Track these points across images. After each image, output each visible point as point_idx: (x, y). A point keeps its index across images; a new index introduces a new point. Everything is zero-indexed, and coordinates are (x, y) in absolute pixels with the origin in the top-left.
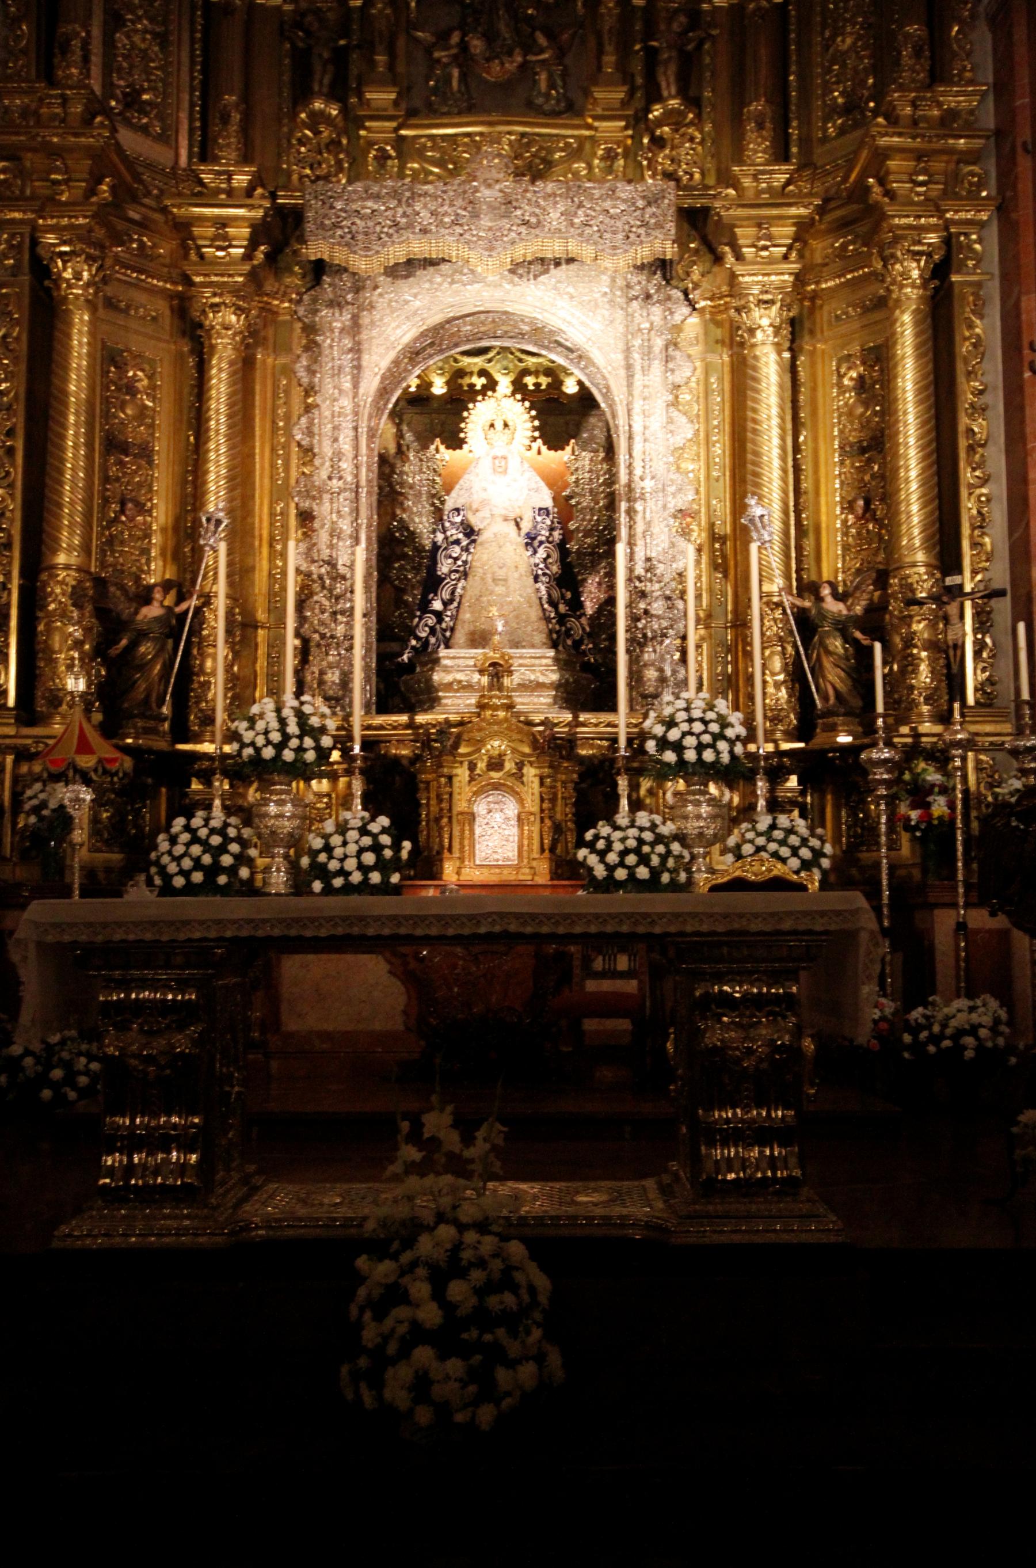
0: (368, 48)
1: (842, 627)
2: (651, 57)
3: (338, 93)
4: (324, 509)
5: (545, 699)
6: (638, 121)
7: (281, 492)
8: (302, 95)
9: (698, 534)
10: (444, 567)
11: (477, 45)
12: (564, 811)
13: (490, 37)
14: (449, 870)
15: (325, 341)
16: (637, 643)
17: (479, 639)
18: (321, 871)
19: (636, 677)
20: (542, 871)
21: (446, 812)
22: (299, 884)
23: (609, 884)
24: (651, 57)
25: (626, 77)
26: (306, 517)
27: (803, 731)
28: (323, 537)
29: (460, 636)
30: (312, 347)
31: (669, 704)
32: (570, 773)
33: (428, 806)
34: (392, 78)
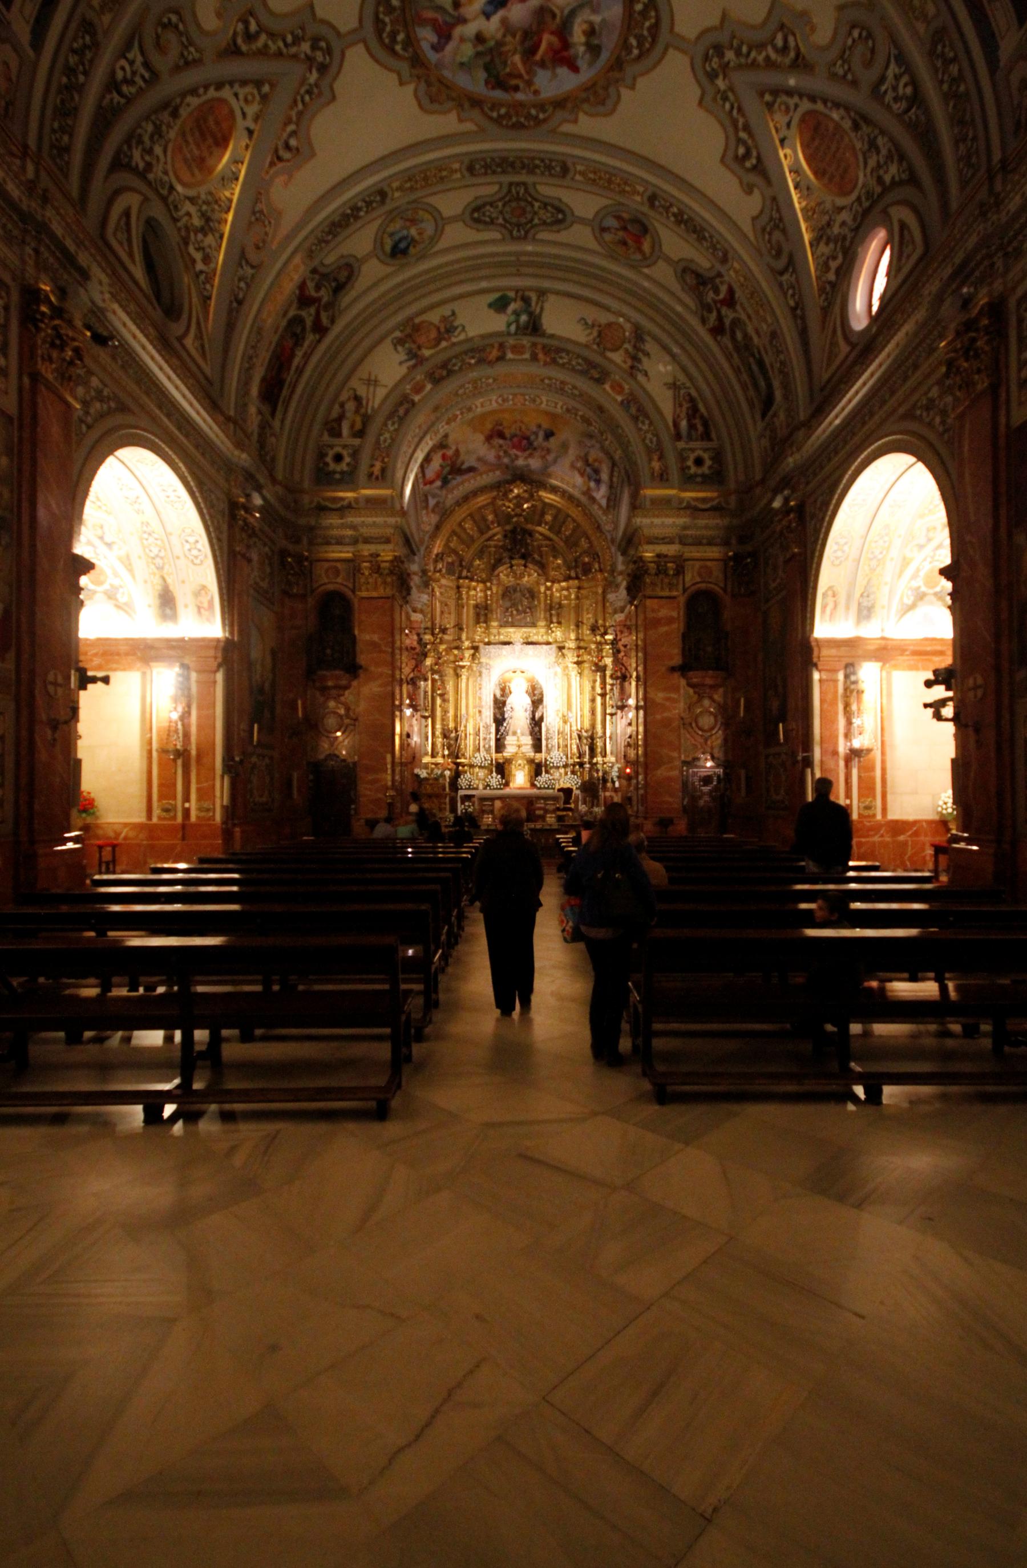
0: (491, 611)
1: (586, 738)
2: (551, 615)
3: (485, 622)
4: (484, 711)
5: (529, 747)
6: (549, 628)
7: (475, 707)
8: (478, 622)
9: (560, 715)
10: (506, 716)
11: (515, 612)
12: (533, 774)
13: (517, 610)
14: (511, 785)
15: (484, 675)
16: (547, 739)
17: (515, 733)
18: (488, 785)
19: (547, 746)
20: (528, 785)
21: (510, 772)
22: (485, 788)
23: (540, 788)
24: (551, 615)
25: (546, 619)
26: (480, 712)
27: (579, 757)
28: (484, 716)
29: (510, 733)
30: (480, 675)
31: (552, 754)
32: (534, 766)
33: (506, 772)
34: (497, 620)
